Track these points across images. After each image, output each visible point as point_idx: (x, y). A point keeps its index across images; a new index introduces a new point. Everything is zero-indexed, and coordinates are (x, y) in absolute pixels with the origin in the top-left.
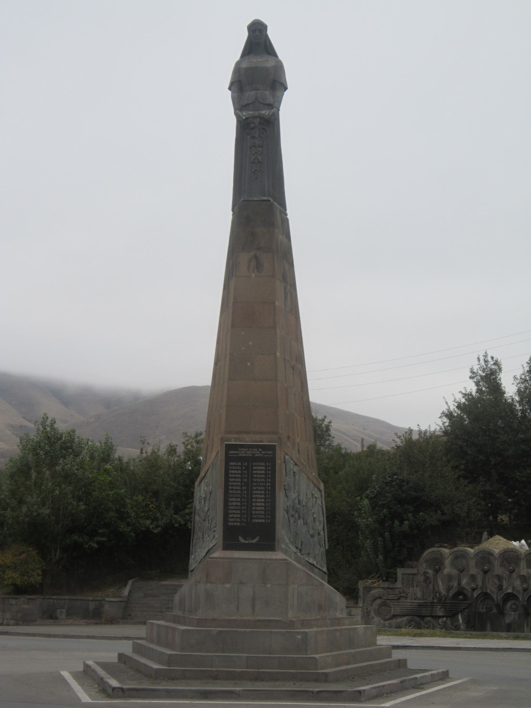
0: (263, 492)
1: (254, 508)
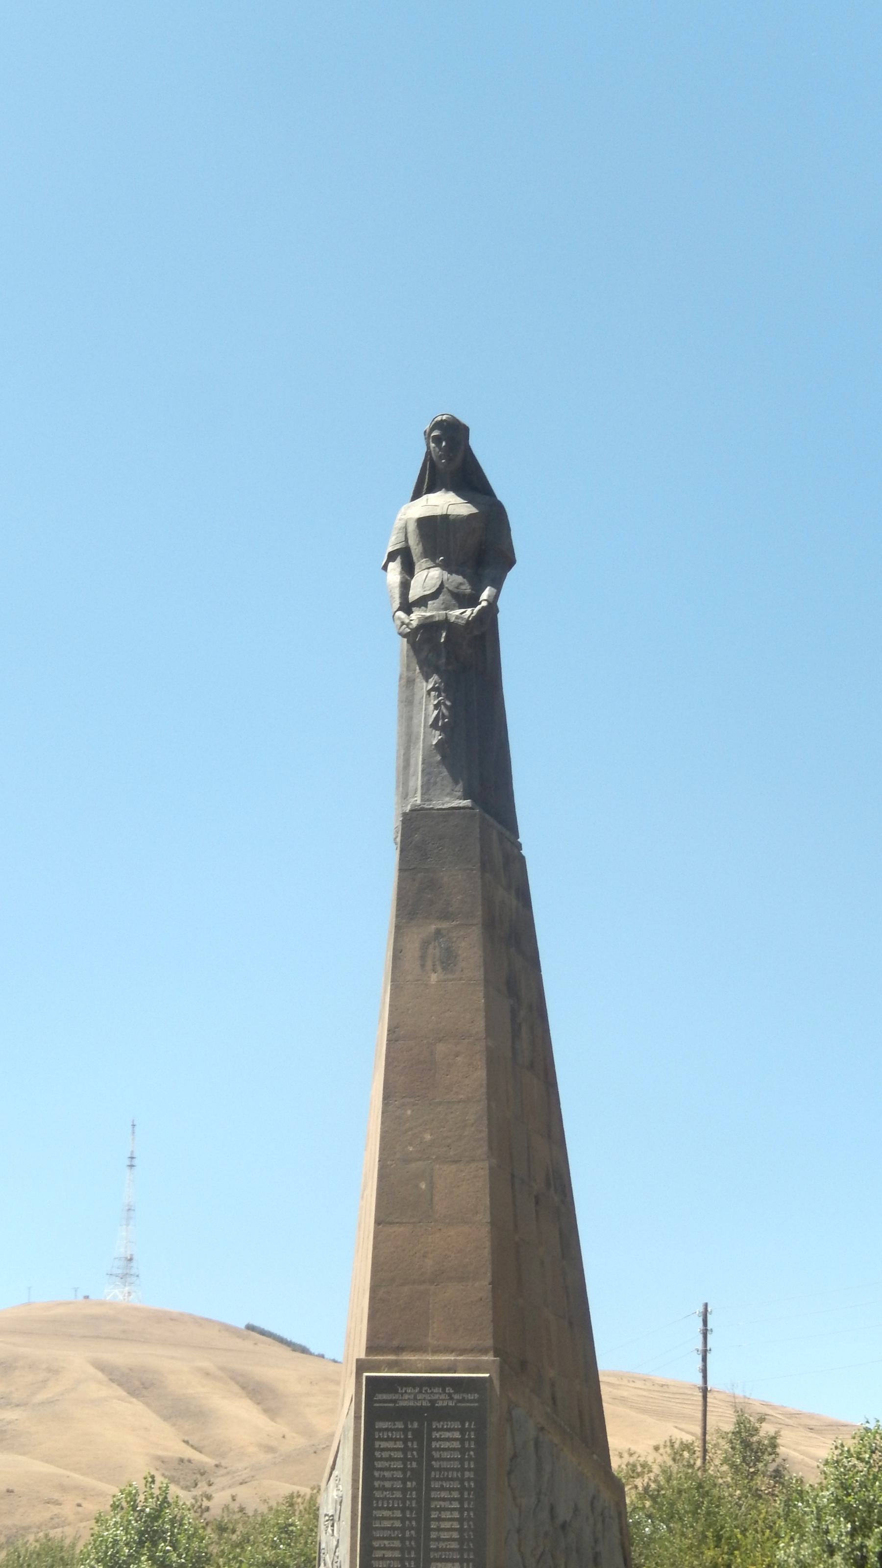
0: (456, 1495)
1: (433, 1535)
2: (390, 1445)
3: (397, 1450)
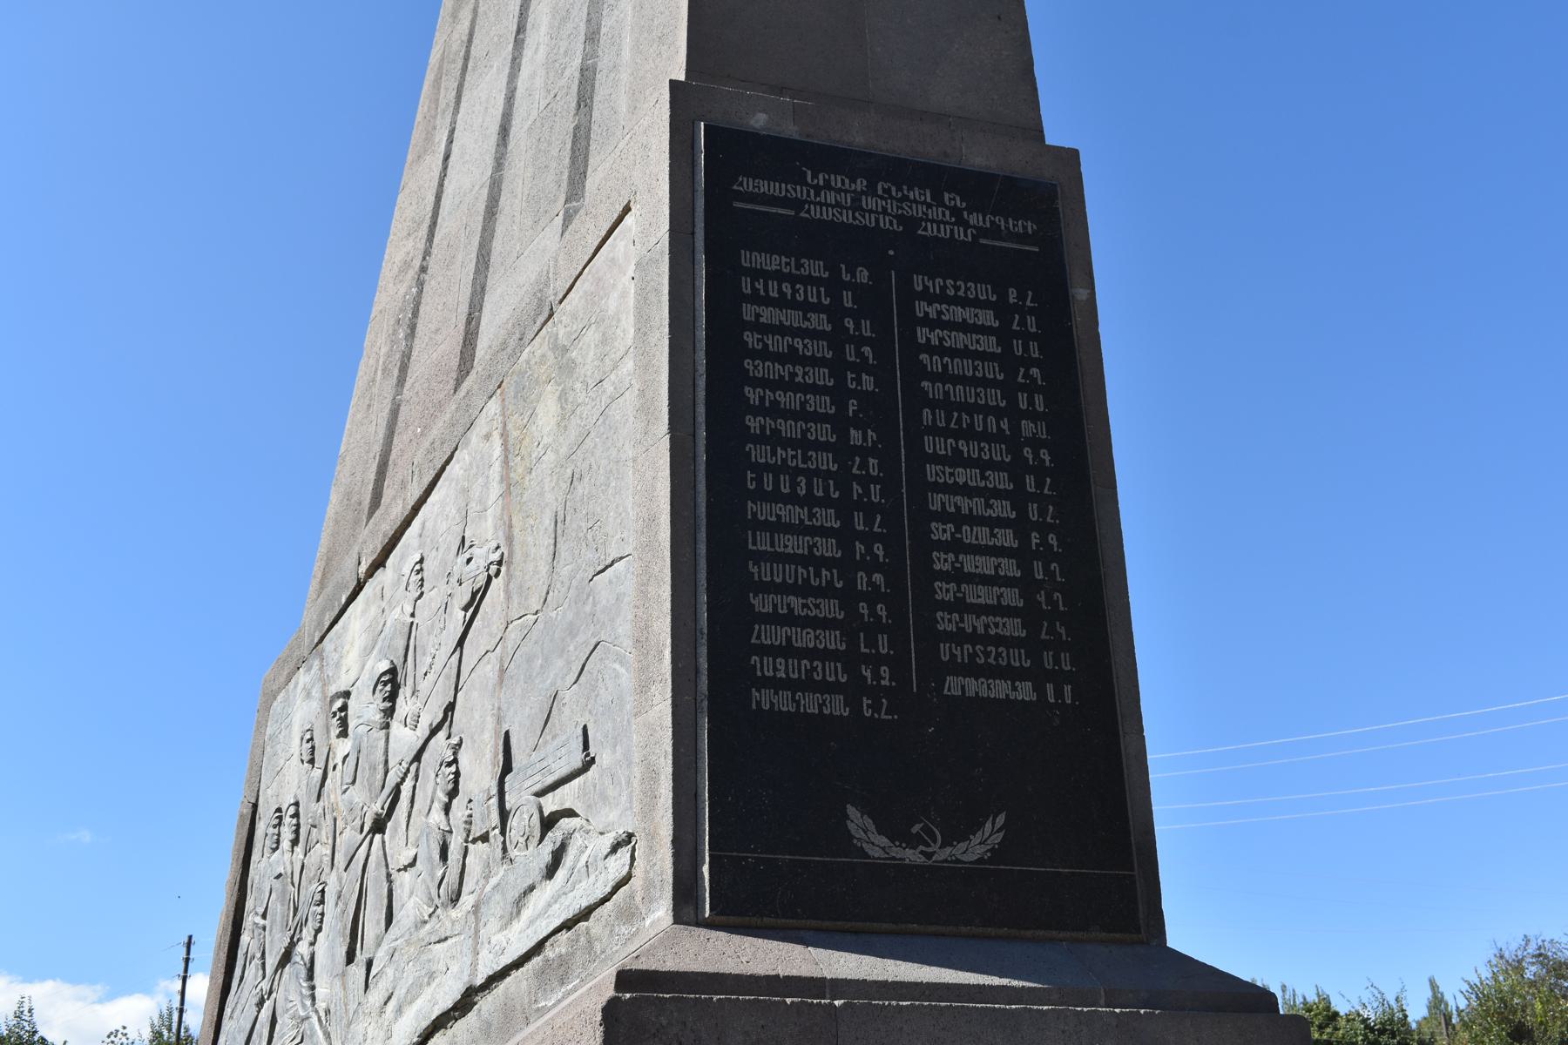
2: (792, 318)
3: (814, 335)
